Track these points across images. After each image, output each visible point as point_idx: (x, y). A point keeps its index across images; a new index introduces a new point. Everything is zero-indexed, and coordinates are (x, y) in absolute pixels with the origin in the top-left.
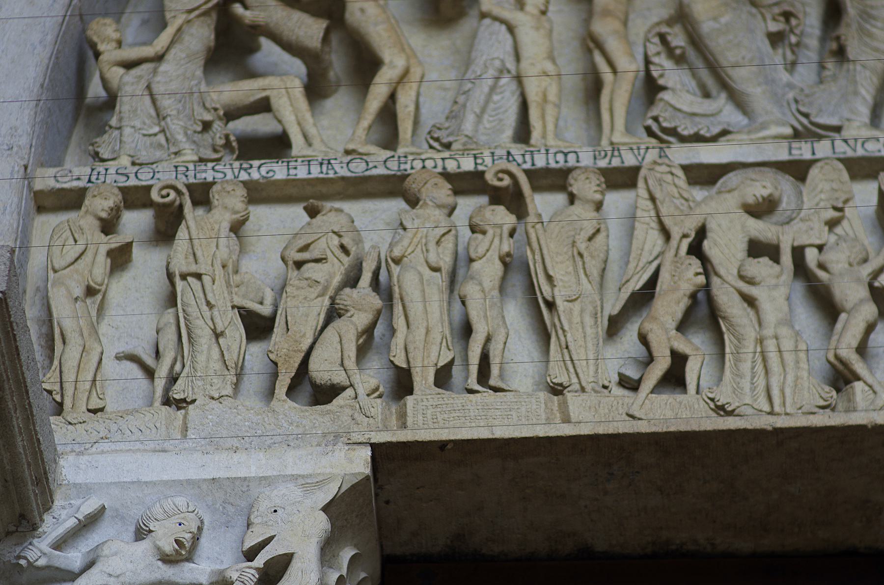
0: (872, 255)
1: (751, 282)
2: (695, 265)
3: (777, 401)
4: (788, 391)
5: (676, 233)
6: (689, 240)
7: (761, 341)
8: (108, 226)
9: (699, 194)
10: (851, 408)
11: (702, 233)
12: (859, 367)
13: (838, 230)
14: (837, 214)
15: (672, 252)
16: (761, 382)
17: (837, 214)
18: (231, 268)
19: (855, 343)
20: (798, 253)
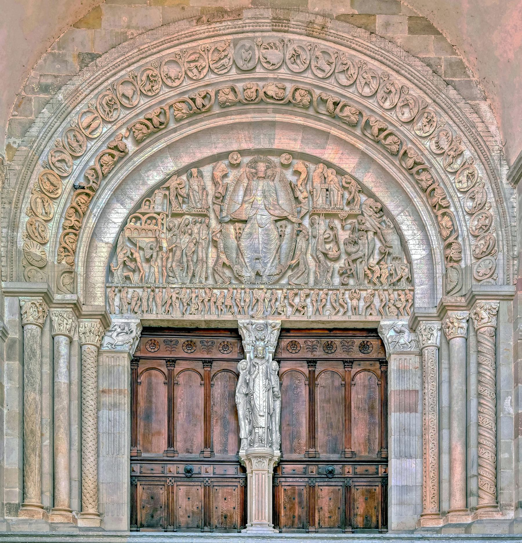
8: (114, 291)
9: (172, 290)
18: (127, 297)
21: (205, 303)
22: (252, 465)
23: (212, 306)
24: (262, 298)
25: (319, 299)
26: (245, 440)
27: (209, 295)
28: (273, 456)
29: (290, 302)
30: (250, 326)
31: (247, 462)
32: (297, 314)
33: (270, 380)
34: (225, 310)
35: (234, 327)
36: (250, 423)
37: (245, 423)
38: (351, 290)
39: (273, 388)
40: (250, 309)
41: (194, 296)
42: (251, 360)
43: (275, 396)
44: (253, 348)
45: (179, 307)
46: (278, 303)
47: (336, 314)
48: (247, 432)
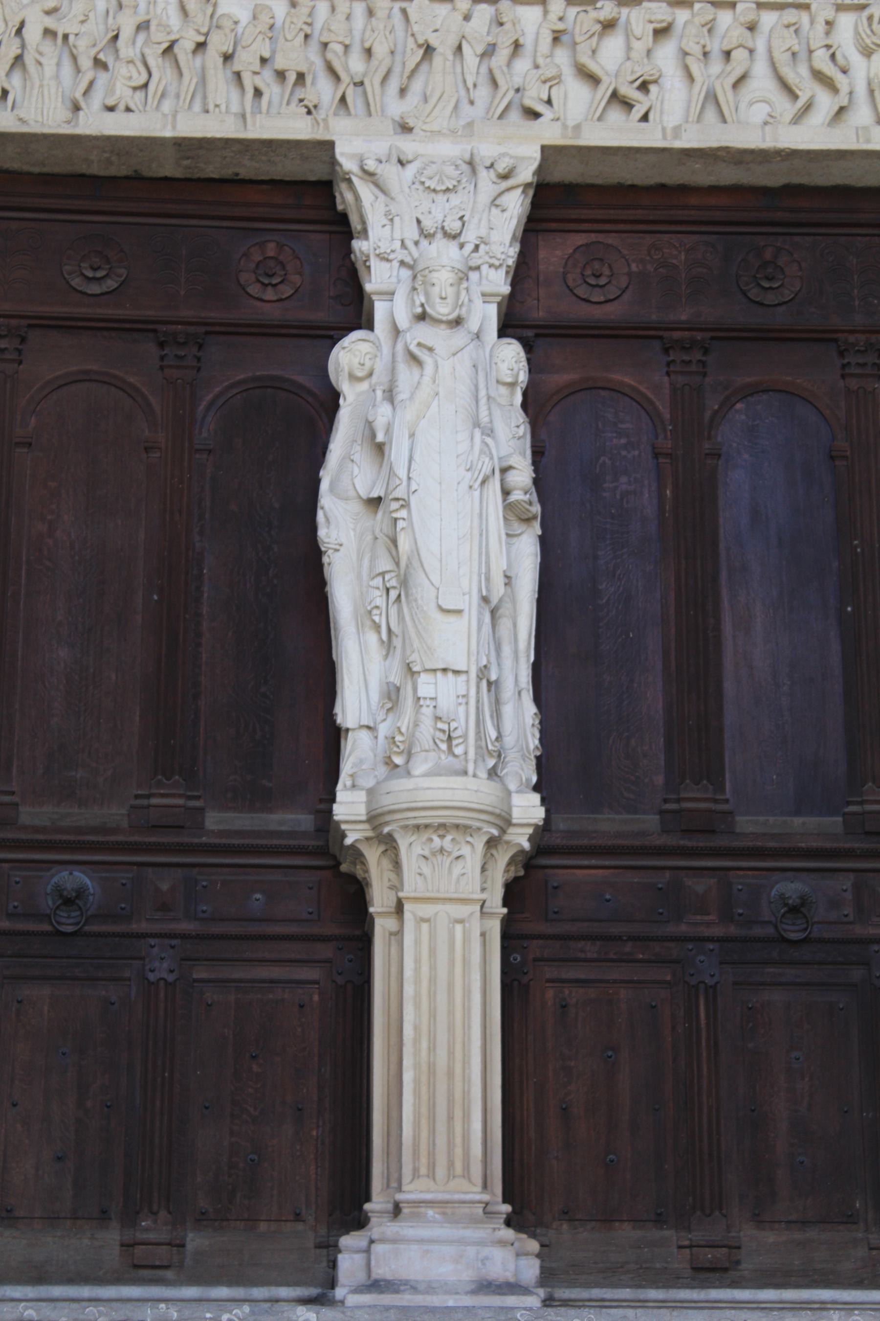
0: (98, 42)
1: (41, 54)
2: (17, 42)
3: (45, 118)
4: (51, 114)
5: (10, 24)
6: (16, 28)
7: (41, 86)
10: (77, 125)
11: (22, 24)
12: (83, 104)
13: (85, 25)
14: (87, 18)
15: (7, 35)
16: (40, 105)
17: (87, 18)
19: (82, 91)
20: (66, 37)
21: (182, 58)
22: (397, 865)
23: (210, 73)
24: (452, 41)
25: (716, 47)
26: (364, 736)
27: (201, 20)
28: (505, 822)
29: (585, 59)
30: (390, 173)
31: (372, 855)
32: (616, 115)
33: (489, 432)
34: (273, 91)
35: (315, 172)
36: (388, 646)
37: (363, 650)
38: (863, 7)
39: (504, 470)
40: (394, 85)
41: (127, 24)
42: (396, 332)
43: (511, 510)
44: (406, 273)
45: (57, 77)
46: (522, 65)
47: (797, 119)
48: (375, 696)
